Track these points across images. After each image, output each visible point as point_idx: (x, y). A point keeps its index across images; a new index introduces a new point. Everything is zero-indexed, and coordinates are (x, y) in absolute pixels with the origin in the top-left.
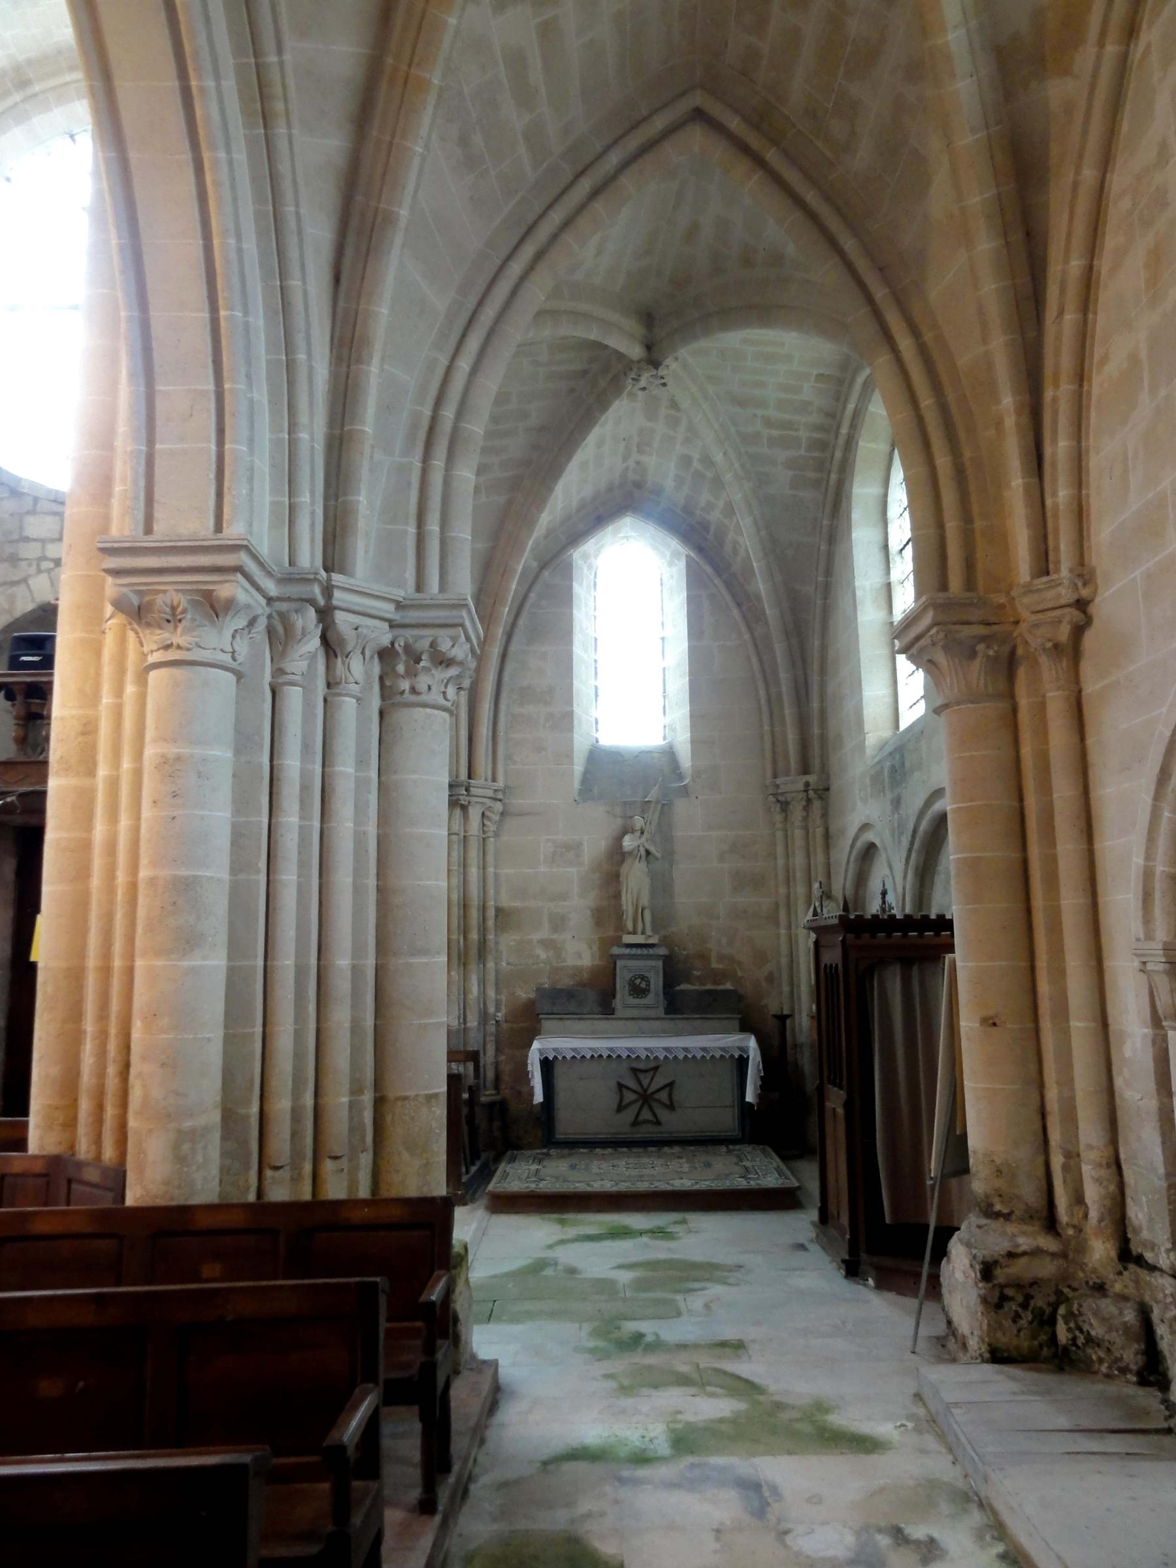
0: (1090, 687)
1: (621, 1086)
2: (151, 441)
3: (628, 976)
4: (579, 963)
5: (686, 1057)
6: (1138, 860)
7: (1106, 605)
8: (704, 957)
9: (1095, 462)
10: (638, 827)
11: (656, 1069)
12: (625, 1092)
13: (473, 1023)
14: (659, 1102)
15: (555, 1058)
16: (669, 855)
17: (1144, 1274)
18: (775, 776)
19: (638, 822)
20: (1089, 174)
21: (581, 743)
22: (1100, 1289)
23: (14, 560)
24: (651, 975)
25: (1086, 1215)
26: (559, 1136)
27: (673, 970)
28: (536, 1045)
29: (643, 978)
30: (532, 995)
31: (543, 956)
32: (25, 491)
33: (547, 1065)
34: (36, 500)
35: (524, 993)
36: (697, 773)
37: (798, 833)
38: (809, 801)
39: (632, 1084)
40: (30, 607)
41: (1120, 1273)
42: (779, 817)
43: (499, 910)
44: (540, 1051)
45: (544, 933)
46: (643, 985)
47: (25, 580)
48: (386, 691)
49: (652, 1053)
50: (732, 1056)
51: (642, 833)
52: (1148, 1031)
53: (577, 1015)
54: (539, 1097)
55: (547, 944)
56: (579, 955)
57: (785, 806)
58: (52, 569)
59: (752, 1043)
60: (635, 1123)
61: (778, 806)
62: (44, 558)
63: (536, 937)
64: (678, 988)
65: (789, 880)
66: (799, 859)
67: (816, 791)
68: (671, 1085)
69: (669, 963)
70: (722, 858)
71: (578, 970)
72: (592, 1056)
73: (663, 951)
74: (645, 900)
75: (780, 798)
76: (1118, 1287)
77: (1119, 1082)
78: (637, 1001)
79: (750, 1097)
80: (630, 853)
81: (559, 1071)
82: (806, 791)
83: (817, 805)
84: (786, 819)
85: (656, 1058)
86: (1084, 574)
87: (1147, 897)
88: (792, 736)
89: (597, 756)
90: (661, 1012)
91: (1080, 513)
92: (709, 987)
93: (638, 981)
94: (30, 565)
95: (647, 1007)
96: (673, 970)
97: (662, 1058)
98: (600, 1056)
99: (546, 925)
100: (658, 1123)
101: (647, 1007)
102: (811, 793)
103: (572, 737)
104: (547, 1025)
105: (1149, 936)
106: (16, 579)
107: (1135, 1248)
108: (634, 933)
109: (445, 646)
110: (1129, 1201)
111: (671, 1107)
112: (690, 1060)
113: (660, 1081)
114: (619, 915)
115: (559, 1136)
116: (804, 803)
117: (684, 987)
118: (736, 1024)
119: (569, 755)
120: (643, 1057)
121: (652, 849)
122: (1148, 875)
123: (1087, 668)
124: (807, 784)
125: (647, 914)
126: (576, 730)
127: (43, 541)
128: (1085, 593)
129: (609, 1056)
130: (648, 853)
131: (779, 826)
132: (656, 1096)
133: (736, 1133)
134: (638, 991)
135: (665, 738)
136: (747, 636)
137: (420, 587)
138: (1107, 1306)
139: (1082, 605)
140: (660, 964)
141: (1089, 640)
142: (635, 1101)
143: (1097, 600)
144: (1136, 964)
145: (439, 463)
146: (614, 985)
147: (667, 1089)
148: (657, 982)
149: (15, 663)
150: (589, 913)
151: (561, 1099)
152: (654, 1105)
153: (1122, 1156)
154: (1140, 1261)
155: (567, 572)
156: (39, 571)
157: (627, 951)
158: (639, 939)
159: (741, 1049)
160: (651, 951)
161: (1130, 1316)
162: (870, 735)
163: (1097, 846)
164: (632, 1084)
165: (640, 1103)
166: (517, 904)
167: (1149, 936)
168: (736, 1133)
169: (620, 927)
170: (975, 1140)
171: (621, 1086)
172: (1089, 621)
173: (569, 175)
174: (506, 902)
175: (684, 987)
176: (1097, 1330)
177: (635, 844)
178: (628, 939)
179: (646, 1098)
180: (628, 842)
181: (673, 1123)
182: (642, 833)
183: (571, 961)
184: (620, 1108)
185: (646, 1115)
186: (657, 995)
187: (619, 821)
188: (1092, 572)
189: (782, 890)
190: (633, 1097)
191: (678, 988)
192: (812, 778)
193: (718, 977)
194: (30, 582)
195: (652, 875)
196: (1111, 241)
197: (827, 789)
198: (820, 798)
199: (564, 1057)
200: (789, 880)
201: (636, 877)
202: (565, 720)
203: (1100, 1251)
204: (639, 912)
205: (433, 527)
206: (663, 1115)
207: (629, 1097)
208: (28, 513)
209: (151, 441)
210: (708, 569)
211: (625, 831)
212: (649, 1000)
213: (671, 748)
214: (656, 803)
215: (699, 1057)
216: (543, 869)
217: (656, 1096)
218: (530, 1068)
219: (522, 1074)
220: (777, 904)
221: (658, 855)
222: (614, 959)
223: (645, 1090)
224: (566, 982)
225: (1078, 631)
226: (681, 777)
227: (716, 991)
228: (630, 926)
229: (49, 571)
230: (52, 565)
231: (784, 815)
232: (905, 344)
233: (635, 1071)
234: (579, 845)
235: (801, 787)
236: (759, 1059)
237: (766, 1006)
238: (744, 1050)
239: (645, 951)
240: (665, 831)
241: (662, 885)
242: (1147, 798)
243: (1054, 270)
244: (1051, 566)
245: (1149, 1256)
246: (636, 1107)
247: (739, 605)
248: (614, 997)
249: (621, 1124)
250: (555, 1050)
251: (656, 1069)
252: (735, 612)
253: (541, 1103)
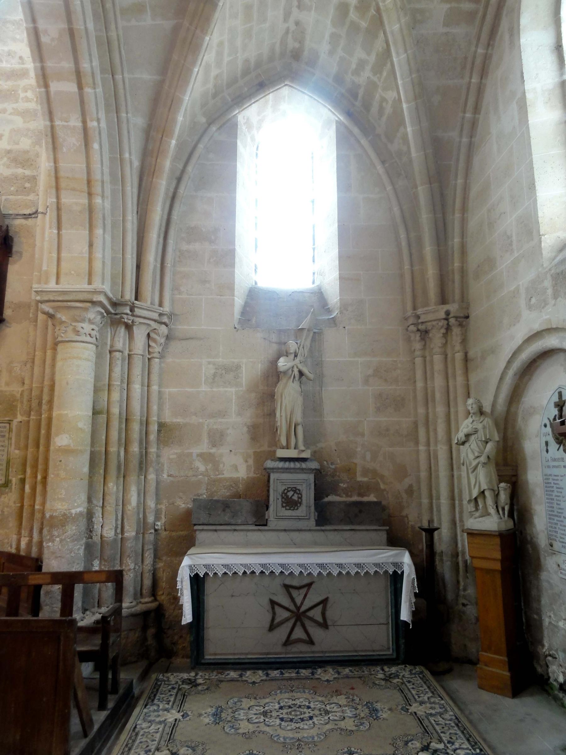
1: (273, 603)
3: (281, 488)
4: (235, 475)
5: (340, 573)
8: (350, 470)
10: (292, 350)
11: (309, 585)
12: (278, 610)
13: (130, 533)
14: (311, 619)
15: (206, 574)
16: (320, 378)
18: (415, 308)
19: (292, 345)
24: (303, 488)
26: (208, 657)
28: (186, 561)
29: (295, 490)
30: (190, 505)
31: (202, 468)
36: (344, 307)
37: (438, 359)
38: (448, 328)
39: (285, 601)
42: (418, 346)
43: (161, 426)
44: (190, 566)
45: (204, 447)
46: (295, 497)
49: (306, 569)
50: (386, 572)
51: (296, 356)
54: (187, 617)
55: (205, 457)
56: (235, 468)
57: (424, 334)
59: (406, 559)
60: (288, 642)
61: (418, 334)
63: (196, 450)
64: (326, 499)
65: (428, 399)
66: (439, 382)
67: (456, 317)
68: (324, 602)
69: (319, 474)
70: (366, 381)
71: (235, 481)
72: (245, 573)
73: (314, 465)
74: (298, 417)
75: (420, 327)
78: (289, 513)
79: (405, 615)
80: (285, 373)
81: (209, 588)
82: (447, 319)
83: (456, 331)
84: (424, 348)
85: (310, 574)
88: (431, 272)
90: (312, 523)
92: (355, 498)
93: (290, 494)
95: (299, 519)
97: (315, 574)
98: (253, 572)
99: (205, 440)
100: (311, 642)
101: (299, 519)
102: (452, 321)
103: (234, 271)
104: (201, 536)
108: (288, 447)
111: (324, 625)
113: (313, 598)
114: (274, 431)
115: (208, 657)
116: (443, 331)
118: (383, 536)
120: (297, 573)
121: (305, 370)
124: (448, 313)
125: (300, 430)
126: (237, 265)
129: (262, 572)
130: (301, 374)
131: (418, 353)
132: (310, 614)
133: (390, 652)
135: (313, 283)
136: (389, 188)
140: (311, 477)
142: (287, 620)
146: (268, 496)
147: (320, 607)
148: (308, 496)
150: (245, 429)
152: (308, 623)
157: (281, 465)
158: (292, 453)
159: (395, 564)
160: (304, 465)
162: (546, 236)
164: (285, 601)
165: (292, 621)
166: (179, 420)
168: (390, 652)
169: (275, 443)
171: (273, 603)
174: (168, 418)
177: (290, 364)
178: (281, 453)
180: (282, 363)
182: (296, 356)
183: (228, 474)
184: (272, 627)
186: (309, 507)
187: (275, 347)
189: (421, 410)
190: (286, 614)
191: (326, 499)
192: (453, 308)
193: (363, 489)
195: (306, 396)
197: (467, 317)
198: (461, 325)
199: (215, 574)
200: (428, 399)
204: (293, 428)
206: (316, 633)
207: (282, 614)
210: (356, 131)
212: (301, 511)
213: (320, 289)
214: (309, 330)
215: (353, 573)
216: (204, 388)
217: (310, 614)
218: (179, 586)
220: (416, 424)
221: (311, 376)
222: (268, 472)
223: (298, 608)
224: (222, 493)
226: (329, 311)
227: (361, 503)
228: (284, 442)
231: (423, 343)
233: (287, 587)
234: (238, 367)
235: (443, 315)
236: (414, 576)
237: (407, 516)
238: (398, 565)
239: (298, 465)
246: (290, 624)
247: (383, 162)
248: (267, 507)
250: (206, 566)
251: (309, 585)
252: (380, 169)
253: (191, 623)
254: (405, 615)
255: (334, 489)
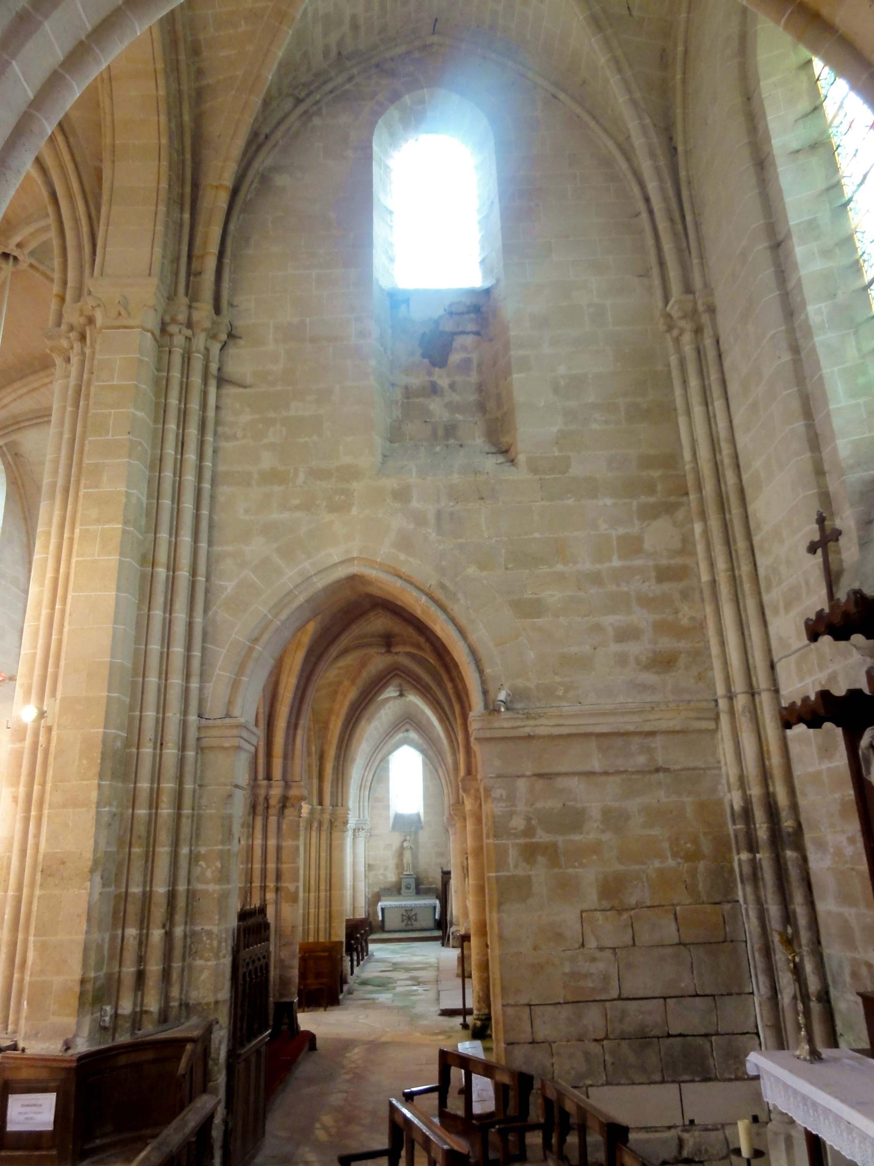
1: (403, 915)
19: (408, 838)
21: (392, 814)
27: (418, 882)
28: (380, 904)
29: (409, 884)
30: (378, 890)
33: (383, 910)
35: (376, 890)
43: (369, 865)
45: (382, 872)
48: (354, 835)
53: (391, 895)
54: (380, 918)
55: (383, 875)
59: (438, 902)
60: (407, 925)
68: (416, 915)
73: (415, 876)
74: (410, 862)
81: (386, 911)
89: (398, 817)
92: (428, 886)
96: (418, 882)
104: (382, 898)
109: (364, 827)
112: (421, 907)
113: (413, 913)
117: (422, 886)
119: (388, 817)
134: (408, 888)
137: (359, 817)
145: (362, 792)
148: (413, 886)
151: (386, 919)
155: (388, 762)
169: (403, 869)
170: (454, 913)
173: (384, 736)
175: (422, 886)
178: (405, 873)
179: (409, 918)
180: (405, 844)
181: (417, 925)
183: (390, 880)
184: (402, 921)
185: (409, 922)
187: (403, 838)
193: (431, 883)
201: (407, 856)
202: (387, 807)
204: (408, 865)
205: (361, 804)
207: (405, 918)
211: (405, 840)
219: (376, 913)
222: (401, 879)
224: (388, 886)
232: (444, 767)
240: (416, 842)
241: (415, 856)
249: (402, 926)
254: (437, 917)
255: (423, 884)
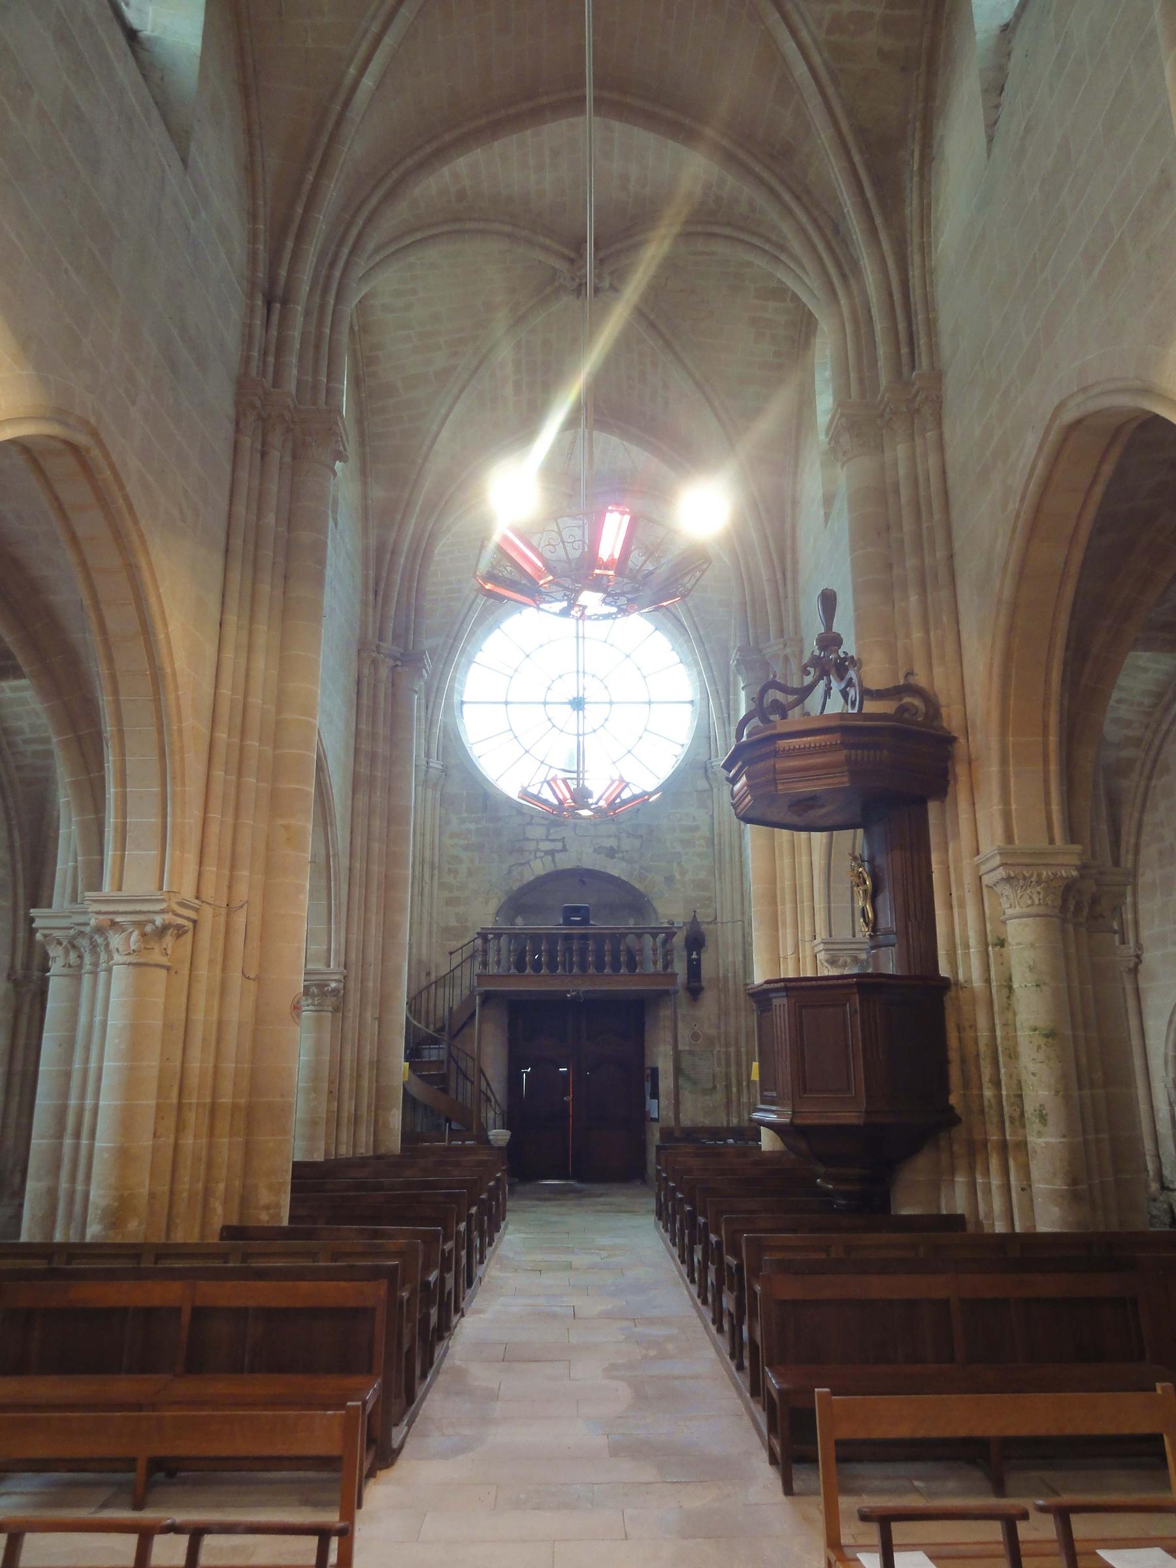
0: (1142, 985)
2: (829, 902)
6: (1163, 1049)
7: (1147, 956)
9: (1140, 907)
17: (1171, 1193)
20: (1136, 815)
22: (1155, 1200)
23: (521, 851)
25: (1148, 1175)
32: (525, 811)
34: (532, 817)
40: (532, 878)
41: (1161, 1194)
47: (528, 863)
52: (1168, 1108)
58: (543, 856)
62: (538, 850)
76: (1161, 1199)
77: (1158, 1127)
86: (1139, 946)
87: (1166, 1063)
91: (1136, 923)
94: (530, 853)
105: (1167, 1075)
106: (523, 862)
107: (1167, 1184)
110: (1163, 1168)
122: (1166, 1055)
123: (1140, 977)
127: (538, 841)
128: (1139, 953)
138: (1158, 1204)
139: (1138, 957)
141: (1140, 967)
143: (1144, 955)
144: (1163, 1084)
149: (567, 922)
153: (1160, 1153)
154: (1169, 1189)
156: (536, 858)
161: (1165, 1206)
163: (1147, 1042)
167: (1167, 1075)
172: (1141, 961)
176: (1155, 1212)
188: (1141, 945)
194: (532, 863)
196: (1145, 838)
203: (1154, 1186)
208: (528, 824)
209: (829, 902)
225: (1137, 965)
229: (541, 858)
230: (543, 854)
242: (1165, 1028)
243: (1124, 837)
244: (1126, 940)
245: (1171, 1186)
